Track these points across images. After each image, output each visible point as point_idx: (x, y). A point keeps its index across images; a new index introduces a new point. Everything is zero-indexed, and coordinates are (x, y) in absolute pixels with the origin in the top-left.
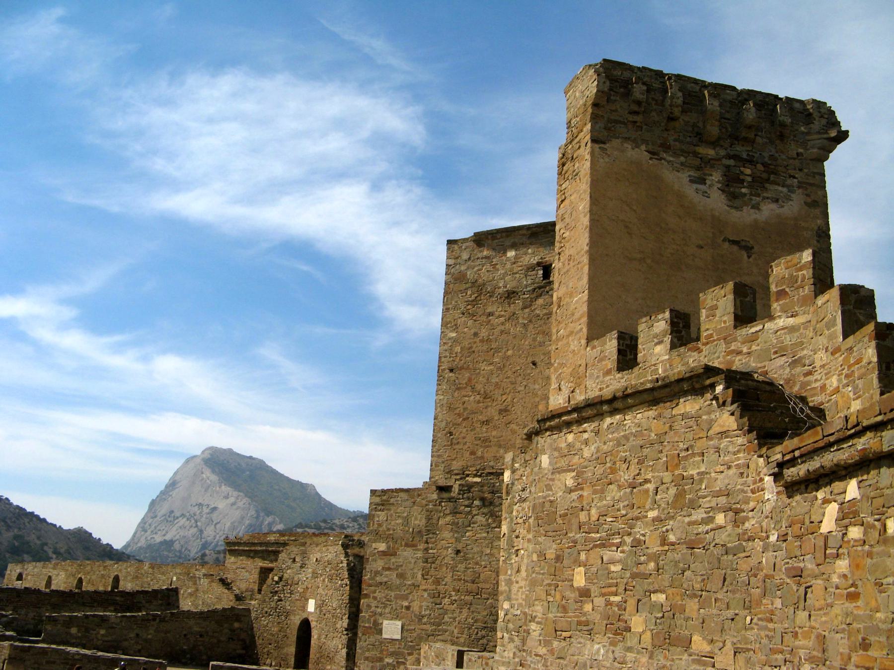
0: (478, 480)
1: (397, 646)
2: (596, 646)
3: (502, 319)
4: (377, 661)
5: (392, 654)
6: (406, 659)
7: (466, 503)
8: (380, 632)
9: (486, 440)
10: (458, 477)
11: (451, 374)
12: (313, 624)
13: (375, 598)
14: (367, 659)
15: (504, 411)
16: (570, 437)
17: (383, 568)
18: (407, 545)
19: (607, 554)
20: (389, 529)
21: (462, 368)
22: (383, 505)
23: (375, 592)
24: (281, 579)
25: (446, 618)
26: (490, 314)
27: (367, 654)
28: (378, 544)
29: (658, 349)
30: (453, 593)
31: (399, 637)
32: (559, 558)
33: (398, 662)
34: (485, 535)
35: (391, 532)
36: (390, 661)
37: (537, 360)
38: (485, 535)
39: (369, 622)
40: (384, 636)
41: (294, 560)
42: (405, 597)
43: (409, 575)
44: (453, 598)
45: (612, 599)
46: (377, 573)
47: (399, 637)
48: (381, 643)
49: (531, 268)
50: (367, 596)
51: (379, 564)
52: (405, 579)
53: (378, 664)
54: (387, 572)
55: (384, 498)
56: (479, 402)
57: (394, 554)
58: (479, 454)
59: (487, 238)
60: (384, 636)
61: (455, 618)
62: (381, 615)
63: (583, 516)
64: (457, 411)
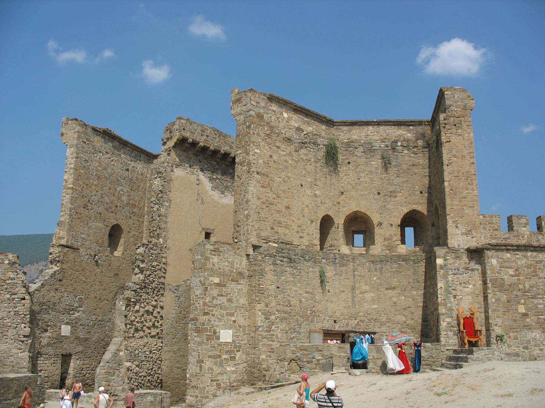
0: (276, 245)
2: (534, 334)
3: (285, 153)
4: (217, 358)
5: (227, 352)
6: (235, 354)
7: (281, 259)
8: (218, 338)
9: (280, 223)
10: (265, 241)
11: (258, 176)
13: (213, 315)
14: (210, 357)
15: (287, 208)
16: (508, 255)
17: (218, 295)
18: (232, 280)
19: (535, 301)
20: (220, 269)
21: (264, 174)
23: (212, 311)
25: (273, 327)
26: (278, 147)
27: (210, 354)
29: (524, 229)
30: (277, 313)
31: (230, 341)
32: (508, 301)
33: (230, 357)
34: (292, 279)
35: (222, 270)
36: (226, 356)
37: (303, 184)
38: (292, 279)
39: (210, 331)
40: (221, 340)
42: (232, 315)
43: (234, 300)
44: (277, 315)
45: (540, 317)
46: (213, 298)
47: (230, 340)
48: (219, 345)
49: (298, 129)
51: (215, 292)
52: (232, 302)
53: (218, 360)
54: (220, 298)
56: (274, 198)
57: (225, 286)
58: (276, 229)
59: (275, 100)
60: (221, 340)
61: (278, 327)
62: (217, 326)
63: (521, 287)
64: (262, 200)
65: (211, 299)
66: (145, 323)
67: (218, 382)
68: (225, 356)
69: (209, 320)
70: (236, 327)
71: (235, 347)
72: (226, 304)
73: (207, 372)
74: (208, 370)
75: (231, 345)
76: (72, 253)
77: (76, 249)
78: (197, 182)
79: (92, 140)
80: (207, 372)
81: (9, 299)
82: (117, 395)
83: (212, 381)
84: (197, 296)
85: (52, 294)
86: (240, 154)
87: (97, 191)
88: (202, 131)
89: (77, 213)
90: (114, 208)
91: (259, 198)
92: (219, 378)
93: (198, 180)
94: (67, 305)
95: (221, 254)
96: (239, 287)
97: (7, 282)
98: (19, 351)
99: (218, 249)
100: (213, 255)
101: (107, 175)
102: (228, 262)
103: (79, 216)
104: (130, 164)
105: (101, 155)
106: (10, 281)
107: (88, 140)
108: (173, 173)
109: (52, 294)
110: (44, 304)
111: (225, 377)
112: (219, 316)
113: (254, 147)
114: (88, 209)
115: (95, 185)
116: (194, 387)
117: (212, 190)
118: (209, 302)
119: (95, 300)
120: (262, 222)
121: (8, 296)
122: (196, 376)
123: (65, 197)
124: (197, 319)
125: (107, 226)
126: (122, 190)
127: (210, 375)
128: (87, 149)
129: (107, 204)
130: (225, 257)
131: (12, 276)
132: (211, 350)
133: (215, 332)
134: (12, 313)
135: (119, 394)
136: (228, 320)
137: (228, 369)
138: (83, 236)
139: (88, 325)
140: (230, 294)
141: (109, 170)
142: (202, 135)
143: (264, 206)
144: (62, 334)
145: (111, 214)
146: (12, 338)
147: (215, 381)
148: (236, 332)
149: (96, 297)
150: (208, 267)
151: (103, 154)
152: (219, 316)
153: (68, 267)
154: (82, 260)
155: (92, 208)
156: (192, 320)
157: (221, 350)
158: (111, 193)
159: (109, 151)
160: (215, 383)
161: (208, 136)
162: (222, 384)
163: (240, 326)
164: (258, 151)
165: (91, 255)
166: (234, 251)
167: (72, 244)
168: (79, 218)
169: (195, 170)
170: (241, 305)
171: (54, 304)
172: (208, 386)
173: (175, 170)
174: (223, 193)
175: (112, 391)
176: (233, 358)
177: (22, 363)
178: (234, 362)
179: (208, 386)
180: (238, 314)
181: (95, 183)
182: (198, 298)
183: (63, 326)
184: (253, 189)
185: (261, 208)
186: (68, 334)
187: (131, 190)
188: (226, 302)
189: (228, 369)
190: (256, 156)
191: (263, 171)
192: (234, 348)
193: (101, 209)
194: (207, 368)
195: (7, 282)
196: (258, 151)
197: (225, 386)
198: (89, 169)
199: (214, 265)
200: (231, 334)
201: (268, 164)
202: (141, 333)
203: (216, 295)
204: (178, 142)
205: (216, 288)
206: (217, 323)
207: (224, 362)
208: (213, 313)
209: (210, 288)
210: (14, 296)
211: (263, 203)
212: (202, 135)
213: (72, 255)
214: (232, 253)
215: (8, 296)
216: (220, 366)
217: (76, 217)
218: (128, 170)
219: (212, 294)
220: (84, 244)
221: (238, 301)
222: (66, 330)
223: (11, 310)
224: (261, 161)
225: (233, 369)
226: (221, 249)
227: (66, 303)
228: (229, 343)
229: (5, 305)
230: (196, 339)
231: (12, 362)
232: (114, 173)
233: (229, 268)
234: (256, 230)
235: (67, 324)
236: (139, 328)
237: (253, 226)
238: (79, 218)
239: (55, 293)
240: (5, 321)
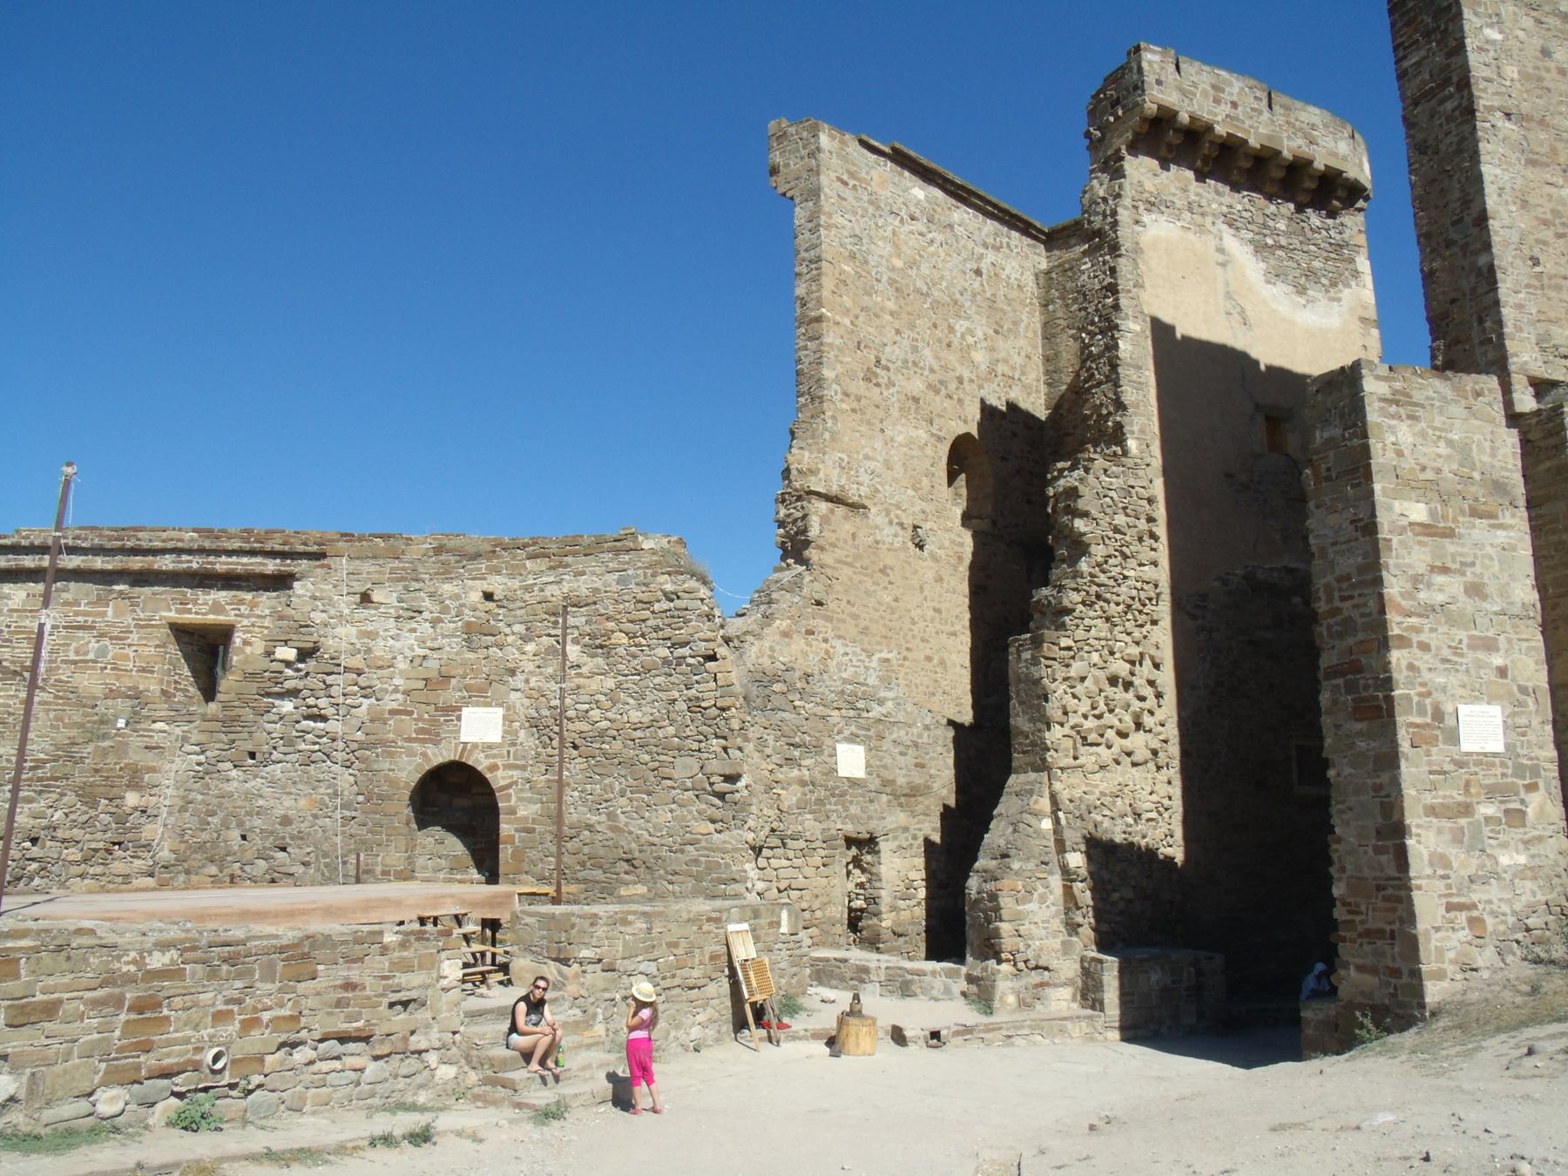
1: (1499, 771)
5: (1492, 792)
6: (1523, 802)
8: (1453, 737)
11: (1508, 124)
12: (498, 779)
13: (1425, 647)
14: (1431, 811)
18: (1474, 513)
22: (1397, 403)
24: (304, 655)
27: (1428, 799)
28: (1406, 504)
31: (1499, 747)
33: (1507, 812)
35: (1429, 475)
40: (1466, 746)
41: (366, 598)
42: (1490, 646)
43: (1491, 589)
46: (1416, 580)
47: (1499, 747)
48: (1460, 765)
50: (1404, 642)
53: (1463, 821)
54: (1439, 579)
55: (1398, 385)
57: (1449, 534)
60: (1466, 746)
62: (1444, 689)
64: (1539, 212)
65: (1409, 586)
66: (1109, 719)
67: (1475, 913)
68: (1488, 810)
69: (1411, 667)
70: (1510, 693)
71: (1519, 771)
72: (1466, 604)
73: (1429, 871)
74: (1431, 864)
75: (1503, 765)
76: (846, 518)
77: (856, 507)
78: (1221, 258)
79: (863, 175)
80: (1429, 871)
81: (665, 661)
82: (1046, 969)
83: (1450, 908)
84: (1348, 577)
85: (798, 643)
86: (1418, 64)
87: (898, 332)
88: (1214, 87)
89: (846, 394)
90: (953, 386)
91: (1524, 204)
92: (1475, 897)
93: (1221, 250)
94: (845, 681)
95: (1420, 412)
96: (1501, 536)
97: (657, 607)
98: (711, 827)
99: (1408, 395)
100: (1392, 417)
101: (920, 284)
102: (1450, 443)
103: (855, 405)
104: (981, 257)
105: (897, 223)
106: (665, 605)
107: (852, 175)
108: (1138, 228)
109: (798, 643)
110: (776, 678)
111: (1494, 892)
112: (1446, 653)
113: (1477, 22)
114: (877, 385)
115: (892, 314)
116: (1371, 934)
117: (1268, 282)
118: (1402, 594)
119: (928, 666)
120: (1553, 294)
121: (663, 652)
122: (1379, 888)
123: (806, 348)
124: (1357, 668)
125: (940, 439)
126: (970, 332)
127: (1440, 885)
128: (854, 202)
129: (932, 371)
130: (1437, 424)
131: (669, 587)
132: (1434, 787)
133: (1438, 715)
134: (681, 706)
135: (1053, 964)
136: (1480, 665)
137: (1505, 860)
138: (872, 465)
139: (916, 745)
140: (1473, 564)
141: (925, 269)
142: (1217, 101)
143: (1548, 234)
144: (842, 772)
145: (947, 403)
146: (689, 784)
147: (1460, 907)
148: (1513, 715)
149: (929, 659)
150: (1381, 460)
151: (902, 220)
152: (1446, 653)
153: (839, 561)
154: (877, 542)
155: (891, 384)
156: (1334, 672)
157: (1467, 784)
158: (940, 341)
159: (918, 214)
160: (1462, 917)
161: (1234, 105)
162: (1490, 922)
163: (1523, 690)
164: (1494, 35)
165: (901, 525)
166: (1463, 402)
167: (842, 488)
168: (854, 411)
169: (1209, 220)
170: (1516, 610)
171: (807, 676)
172: (1437, 929)
173: (1146, 218)
174: (1302, 291)
175: (1030, 954)
176: (1516, 817)
177: (727, 866)
178: (1517, 833)
179: (1437, 929)
180: (1509, 641)
181: (891, 305)
182: (1353, 586)
183: (839, 746)
184: (1498, 171)
185: (1538, 241)
186: (859, 773)
187: (997, 332)
188: (1462, 597)
189: (1505, 860)
190: (1492, 54)
191: (1525, 107)
192: (1515, 775)
193: (917, 386)
194: (1425, 853)
195: (657, 607)
196: (1494, 35)
197: (1502, 928)
198: (866, 262)
199: (1400, 454)
200: (1499, 720)
201: (1540, 79)
202: (1105, 754)
203: (1421, 568)
204: (1146, 127)
205: (1420, 543)
206: (1441, 680)
207: (1486, 831)
208: (1423, 637)
209: (1401, 542)
210: (686, 651)
211: (1545, 223)
212: (1217, 101)
213: (848, 527)
214: (1457, 410)
215: (663, 652)
216: (1471, 848)
217: (844, 406)
218: (978, 272)
219: (1410, 566)
220: (877, 491)
221: (1504, 592)
222: (851, 760)
223: (677, 695)
224: (1511, 71)
225: (1522, 859)
226: (1417, 396)
227: (844, 675)
228: (1495, 755)
229: (658, 680)
230: (1362, 745)
231: (696, 862)
232: (942, 278)
233: (1455, 466)
234: (1531, 323)
235: (853, 738)
236: (1092, 737)
237: (1519, 307)
238: (854, 411)
239: (809, 645)
240: (661, 733)
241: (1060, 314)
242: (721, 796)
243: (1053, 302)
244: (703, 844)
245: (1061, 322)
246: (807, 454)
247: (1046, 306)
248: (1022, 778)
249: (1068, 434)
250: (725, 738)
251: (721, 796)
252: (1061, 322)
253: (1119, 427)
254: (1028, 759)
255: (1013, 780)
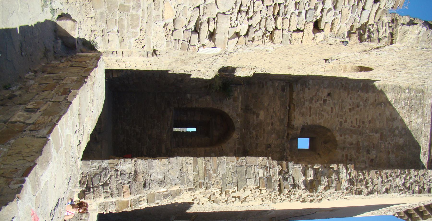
241: (403, 96)
242: (196, 30)
243: (409, 92)
244: (154, 13)
245: (399, 96)
246: (414, 37)
247: (408, 89)
248: (190, 168)
249: (348, 94)
250: (247, 34)
251: (196, 30)
252: (399, 96)
253: (360, 193)
254: (201, 172)
255: (190, 159)
